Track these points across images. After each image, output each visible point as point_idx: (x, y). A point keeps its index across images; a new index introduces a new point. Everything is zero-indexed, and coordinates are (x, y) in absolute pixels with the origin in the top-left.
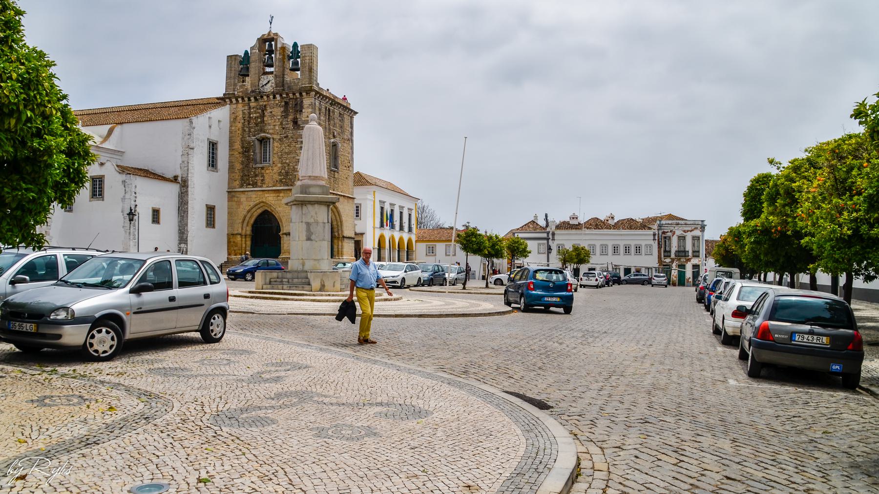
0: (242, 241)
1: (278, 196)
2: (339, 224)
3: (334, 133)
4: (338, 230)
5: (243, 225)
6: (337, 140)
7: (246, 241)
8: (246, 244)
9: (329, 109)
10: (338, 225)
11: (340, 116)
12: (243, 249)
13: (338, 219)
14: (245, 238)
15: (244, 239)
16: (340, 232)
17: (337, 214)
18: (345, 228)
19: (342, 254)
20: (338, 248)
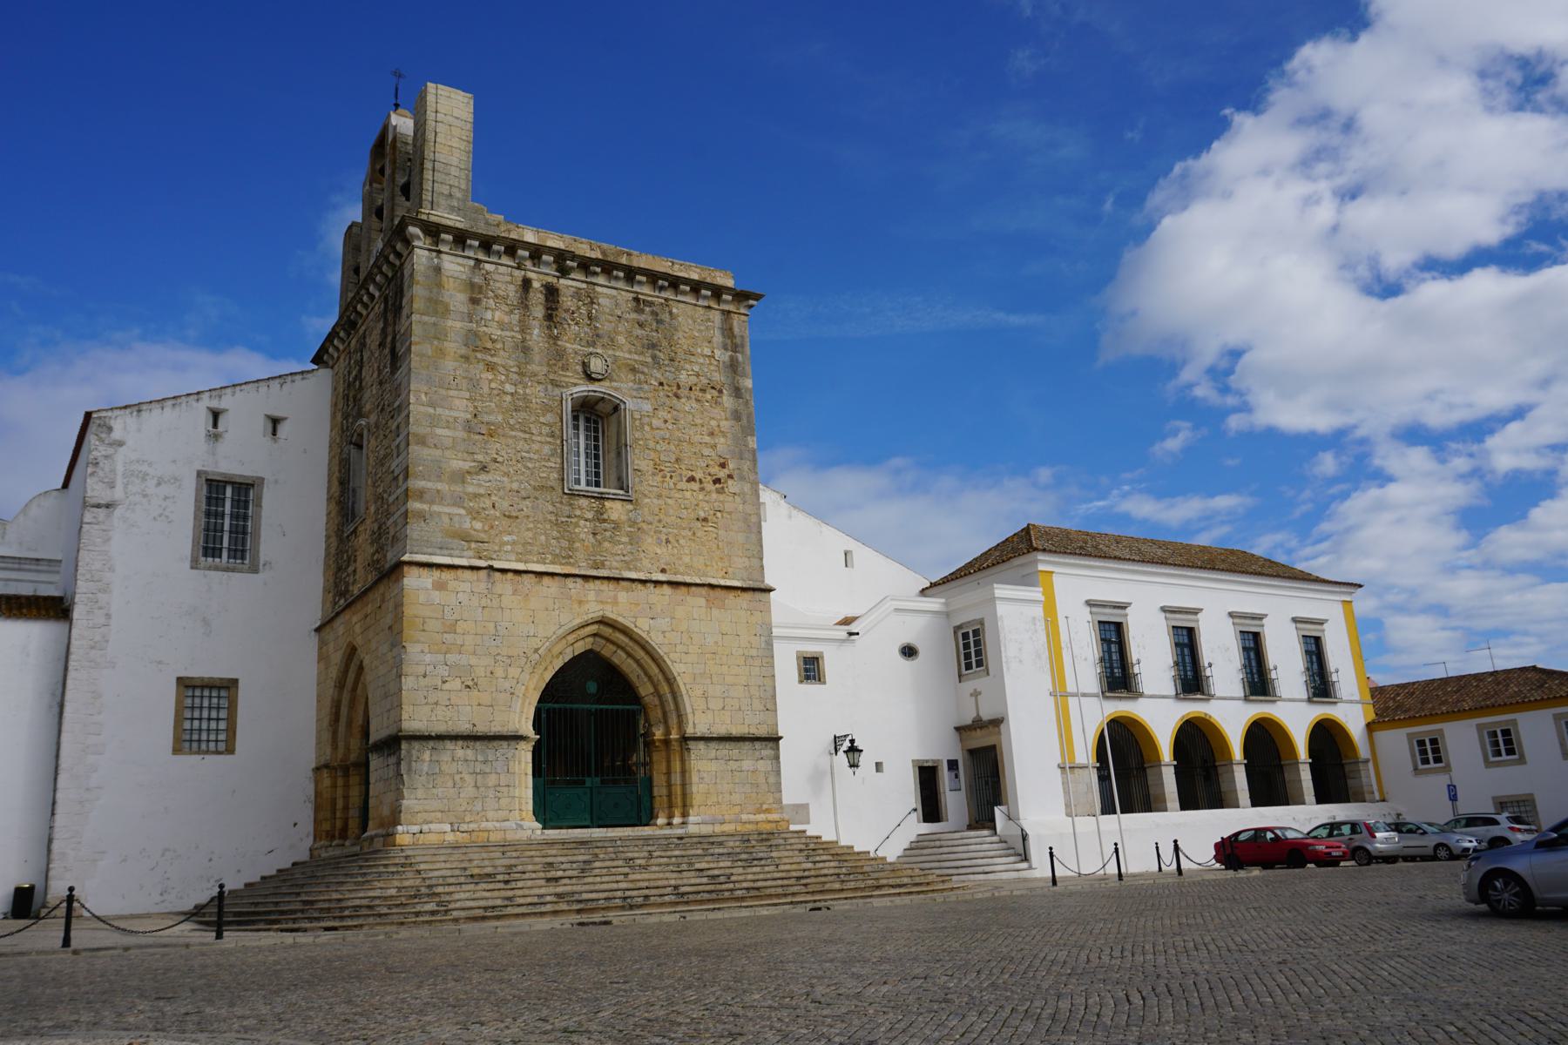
0: (334, 786)
1: (366, 616)
2: (665, 689)
3: (585, 365)
4: (665, 714)
5: (335, 733)
6: (620, 389)
7: (347, 786)
8: (346, 797)
9: (551, 292)
10: (660, 697)
11: (639, 311)
12: (338, 814)
13: (654, 670)
14: (346, 775)
15: (340, 782)
16: (673, 721)
17: (640, 654)
18: (689, 703)
19: (684, 806)
20: (669, 786)
